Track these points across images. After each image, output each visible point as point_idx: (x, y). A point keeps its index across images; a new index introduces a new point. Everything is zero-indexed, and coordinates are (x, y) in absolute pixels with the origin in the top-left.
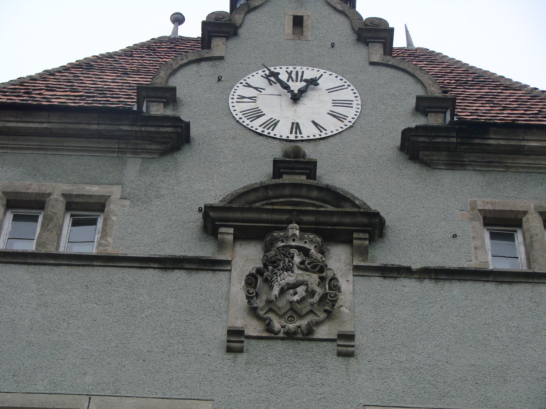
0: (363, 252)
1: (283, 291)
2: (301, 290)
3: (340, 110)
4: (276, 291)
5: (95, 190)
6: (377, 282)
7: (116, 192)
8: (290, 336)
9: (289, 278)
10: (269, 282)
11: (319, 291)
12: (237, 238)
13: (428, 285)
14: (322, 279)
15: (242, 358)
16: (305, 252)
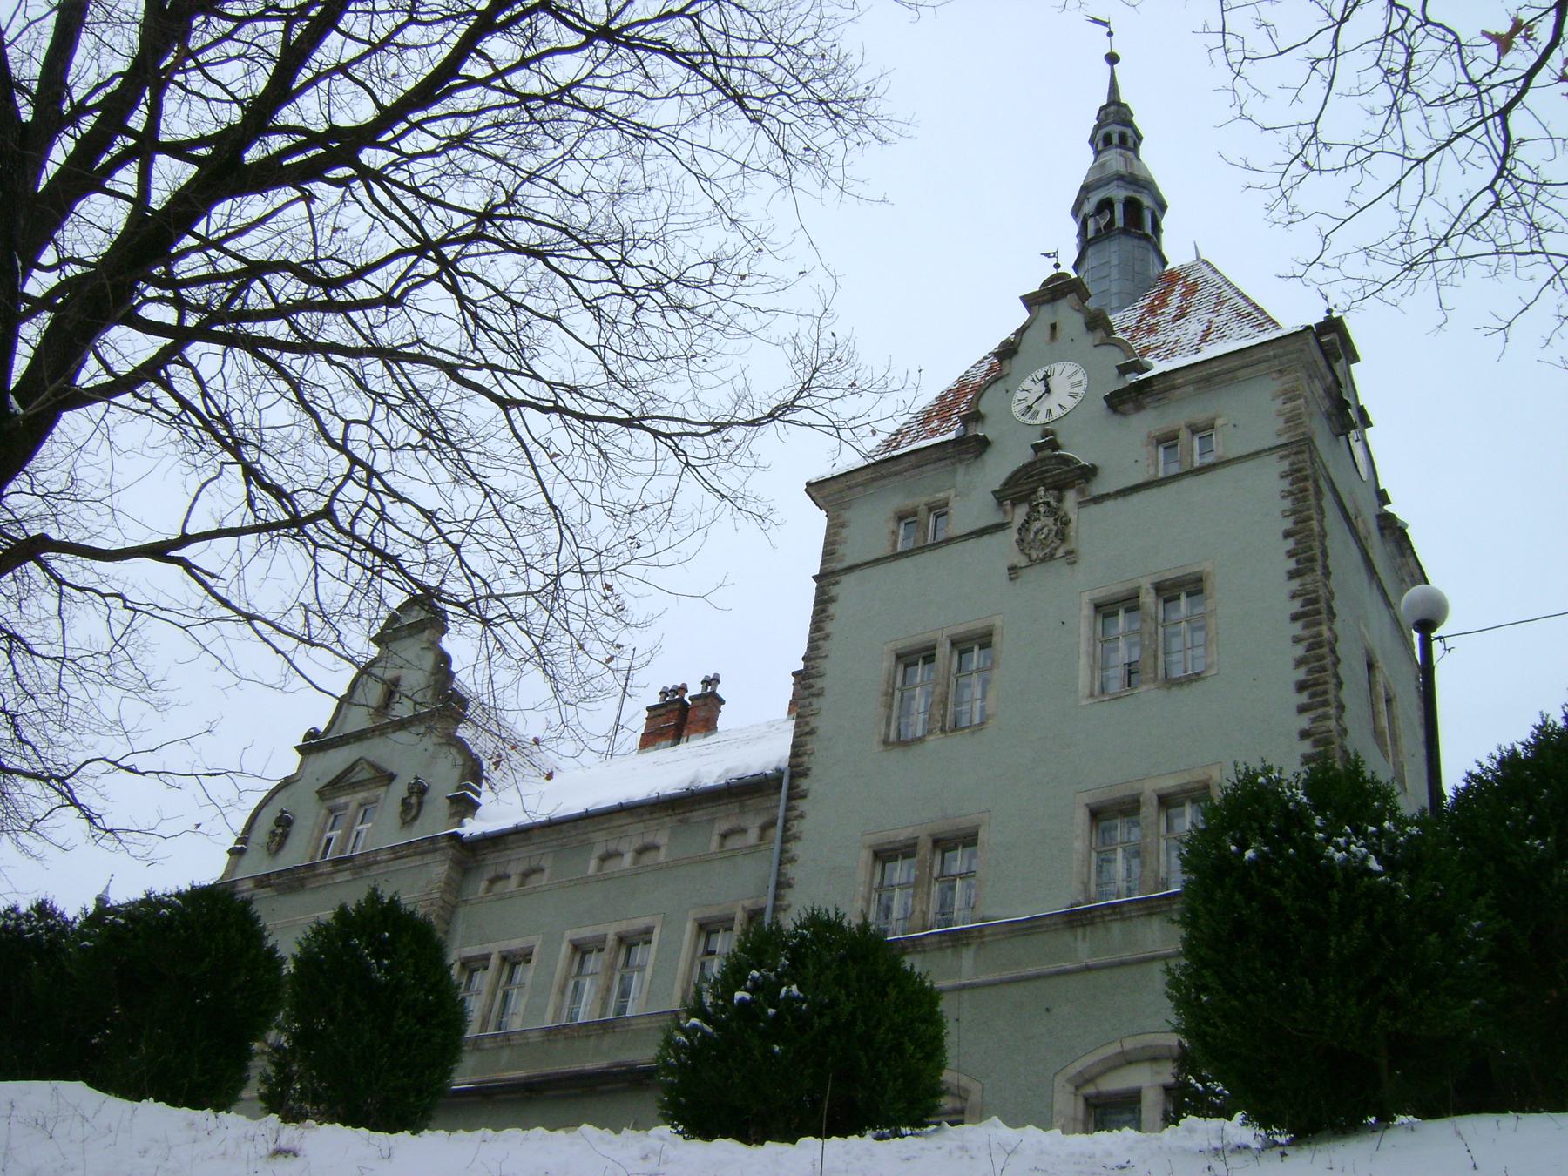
0: (1081, 492)
1: (1036, 534)
2: (1045, 531)
3: (1075, 390)
4: (1032, 535)
5: (941, 495)
6: (1093, 509)
7: (952, 492)
8: (1043, 560)
9: (1037, 525)
10: (1028, 530)
11: (1054, 528)
12: (1014, 505)
13: (1120, 503)
14: (1056, 520)
15: (1018, 581)
16: (1047, 504)
